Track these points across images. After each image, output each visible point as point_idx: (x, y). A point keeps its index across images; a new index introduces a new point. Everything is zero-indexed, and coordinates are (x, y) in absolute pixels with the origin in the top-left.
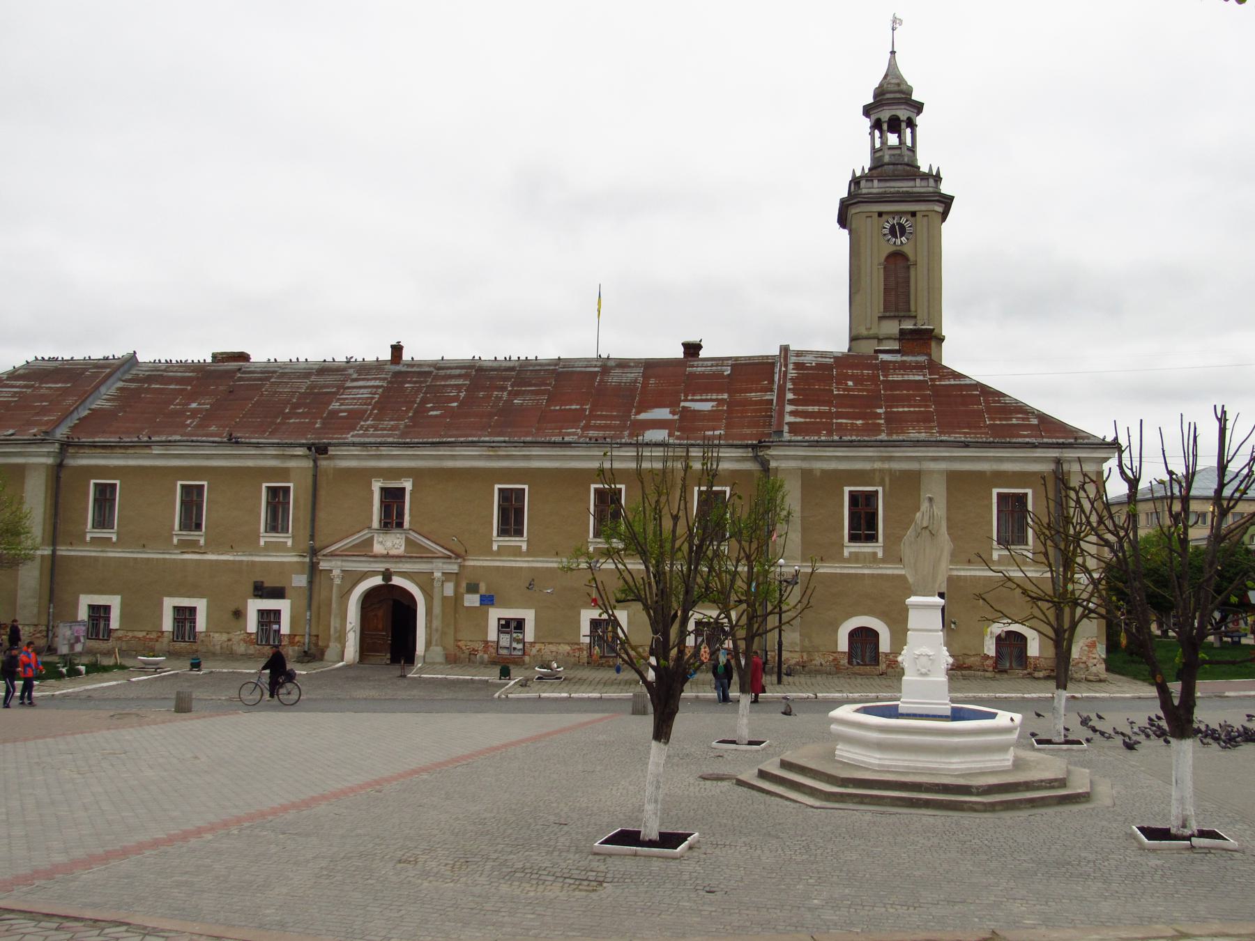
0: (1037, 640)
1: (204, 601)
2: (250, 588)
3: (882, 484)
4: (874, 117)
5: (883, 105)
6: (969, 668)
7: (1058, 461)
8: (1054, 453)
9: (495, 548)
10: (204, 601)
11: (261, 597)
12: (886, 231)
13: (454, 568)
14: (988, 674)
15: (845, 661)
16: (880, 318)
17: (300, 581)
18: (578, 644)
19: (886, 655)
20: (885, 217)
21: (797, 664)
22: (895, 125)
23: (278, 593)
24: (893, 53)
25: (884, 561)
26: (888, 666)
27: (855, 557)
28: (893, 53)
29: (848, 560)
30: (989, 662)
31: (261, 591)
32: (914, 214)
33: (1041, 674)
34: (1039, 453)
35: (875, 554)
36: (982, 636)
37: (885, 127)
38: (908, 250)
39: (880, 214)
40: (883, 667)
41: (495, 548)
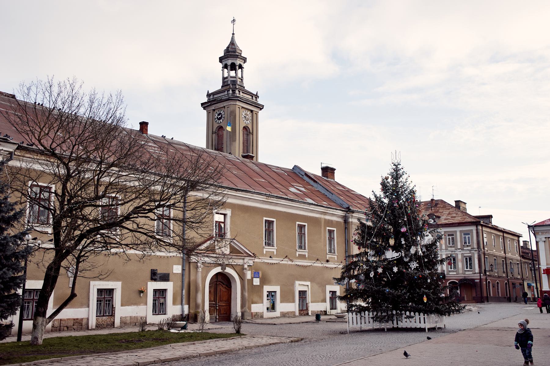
1: (120, 283)
2: (149, 274)
4: (229, 62)
5: (228, 57)
9: (265, 252)
10: (120, 283)
11: (155, 280)
13: (251, 263)
17: (177, 269)
22: (233, 67)
23: (165, 278)
24: (233, 34)
28: (233, 34)
31: (154, 276)
32: (252, 111)
37: (229, 68)
39: (242, 107)
41: (265, 252)
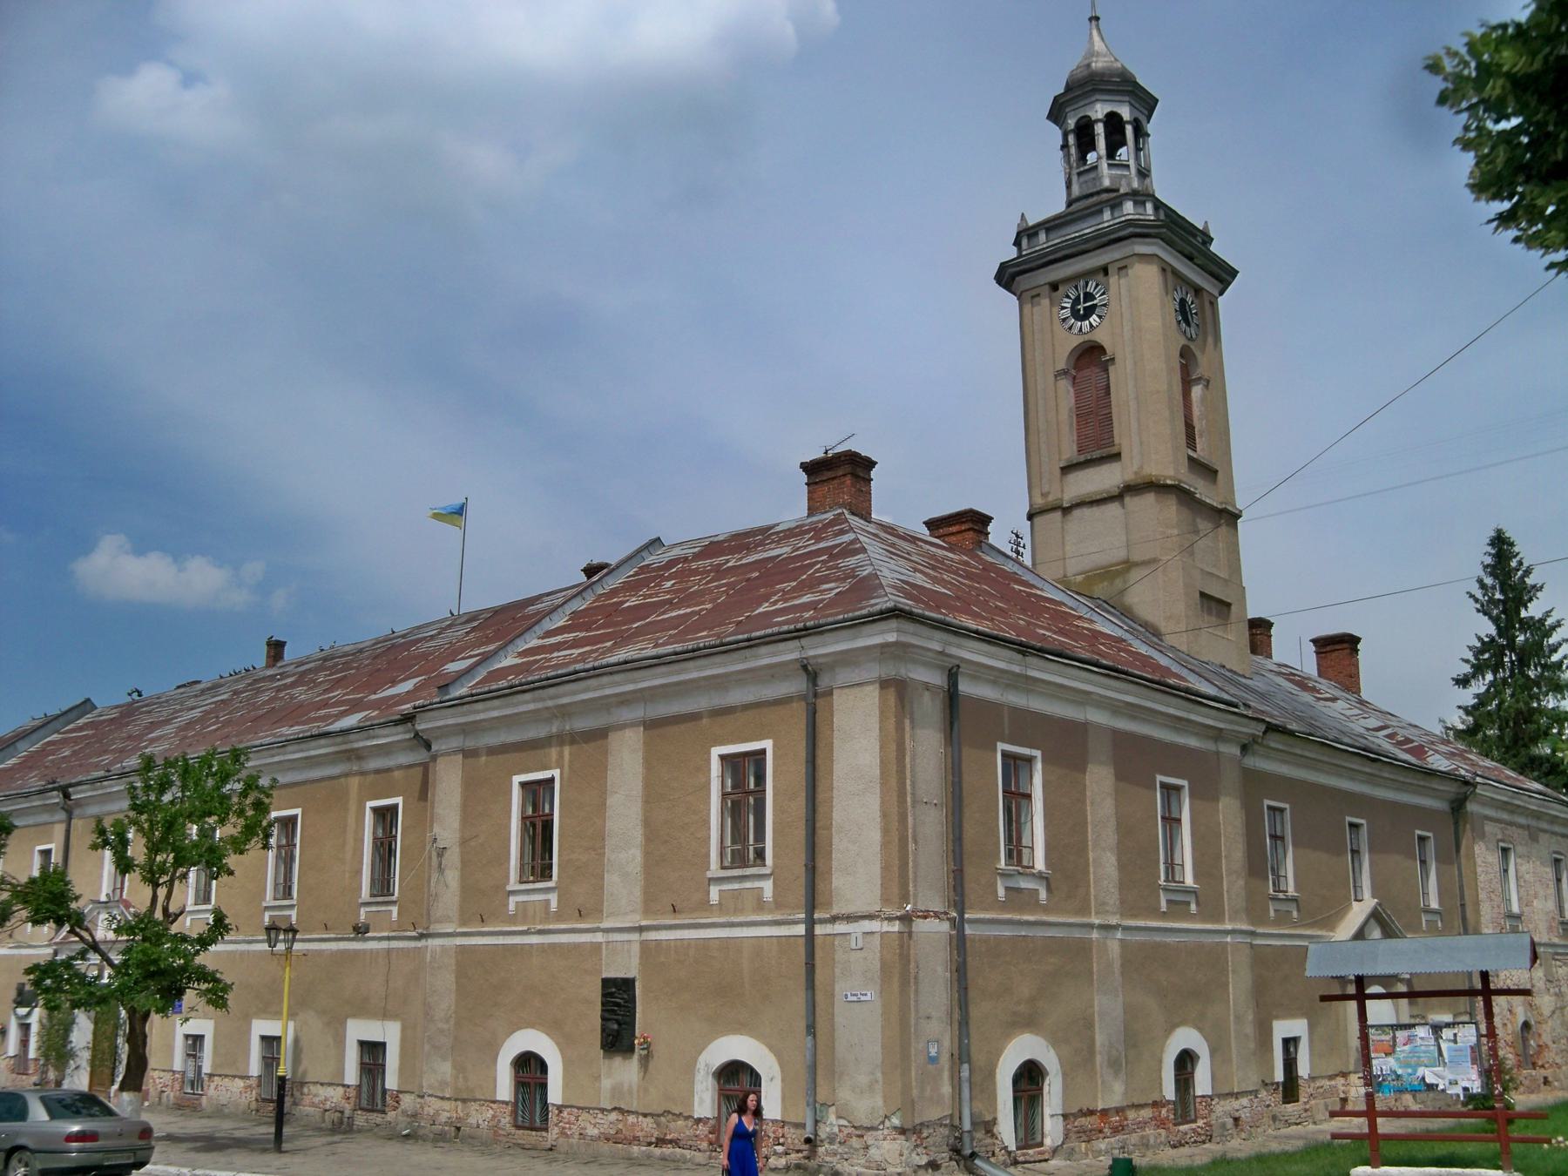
0: (778, 1082)
3: (560, 766)
6: (675, 1142)
7: (811, 672)
8: (789, 653)
12: (1067, 313)
14: (700, 1157)
15: (506, 1121)
16: (1067, 469)
18: (245, 1077)
19: (560, 1108)
20: (1061, 289)
21: (449, 1123)
25: (559, 917)
26: (563, 1133)
27: (523, 912)
29: (512, 919)
30: (702, 1130)
32: (1105, 270)
33: (782, 1162)
34: (766, 657)
35: (547, 902)
36: (690, 1069)
38: (1101, 337)
39: (1054, 287)
40: (553, 1134)
